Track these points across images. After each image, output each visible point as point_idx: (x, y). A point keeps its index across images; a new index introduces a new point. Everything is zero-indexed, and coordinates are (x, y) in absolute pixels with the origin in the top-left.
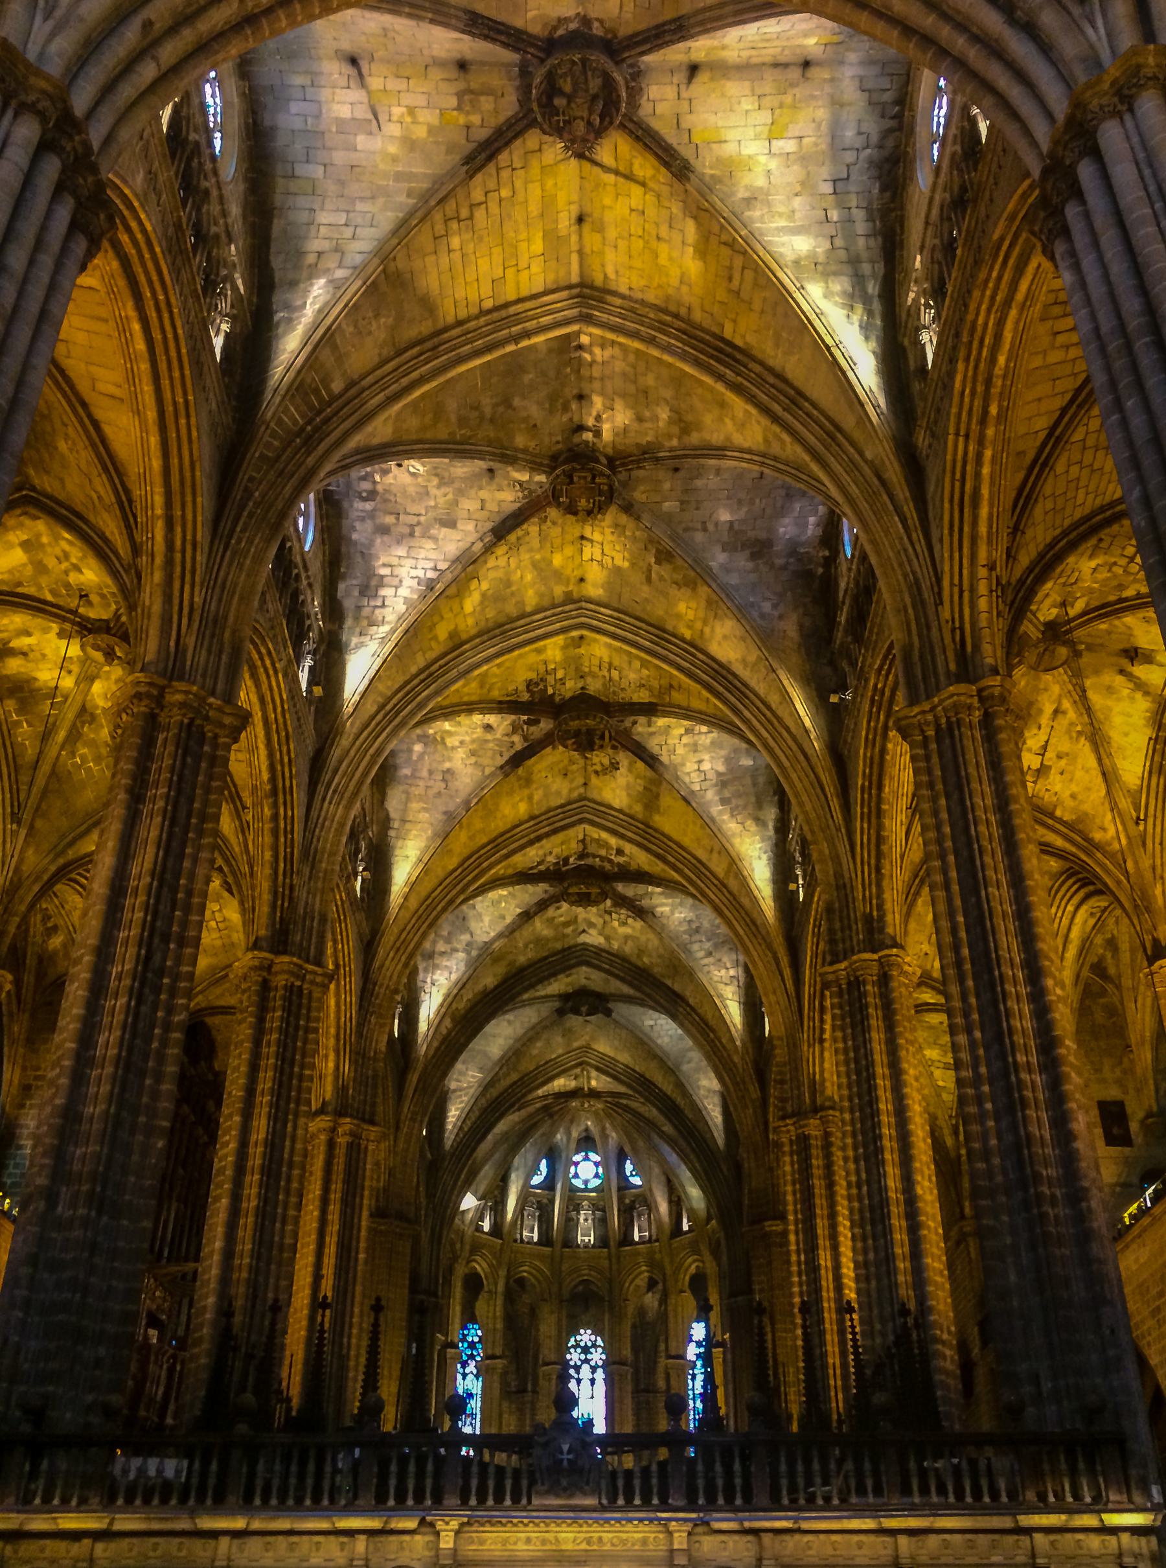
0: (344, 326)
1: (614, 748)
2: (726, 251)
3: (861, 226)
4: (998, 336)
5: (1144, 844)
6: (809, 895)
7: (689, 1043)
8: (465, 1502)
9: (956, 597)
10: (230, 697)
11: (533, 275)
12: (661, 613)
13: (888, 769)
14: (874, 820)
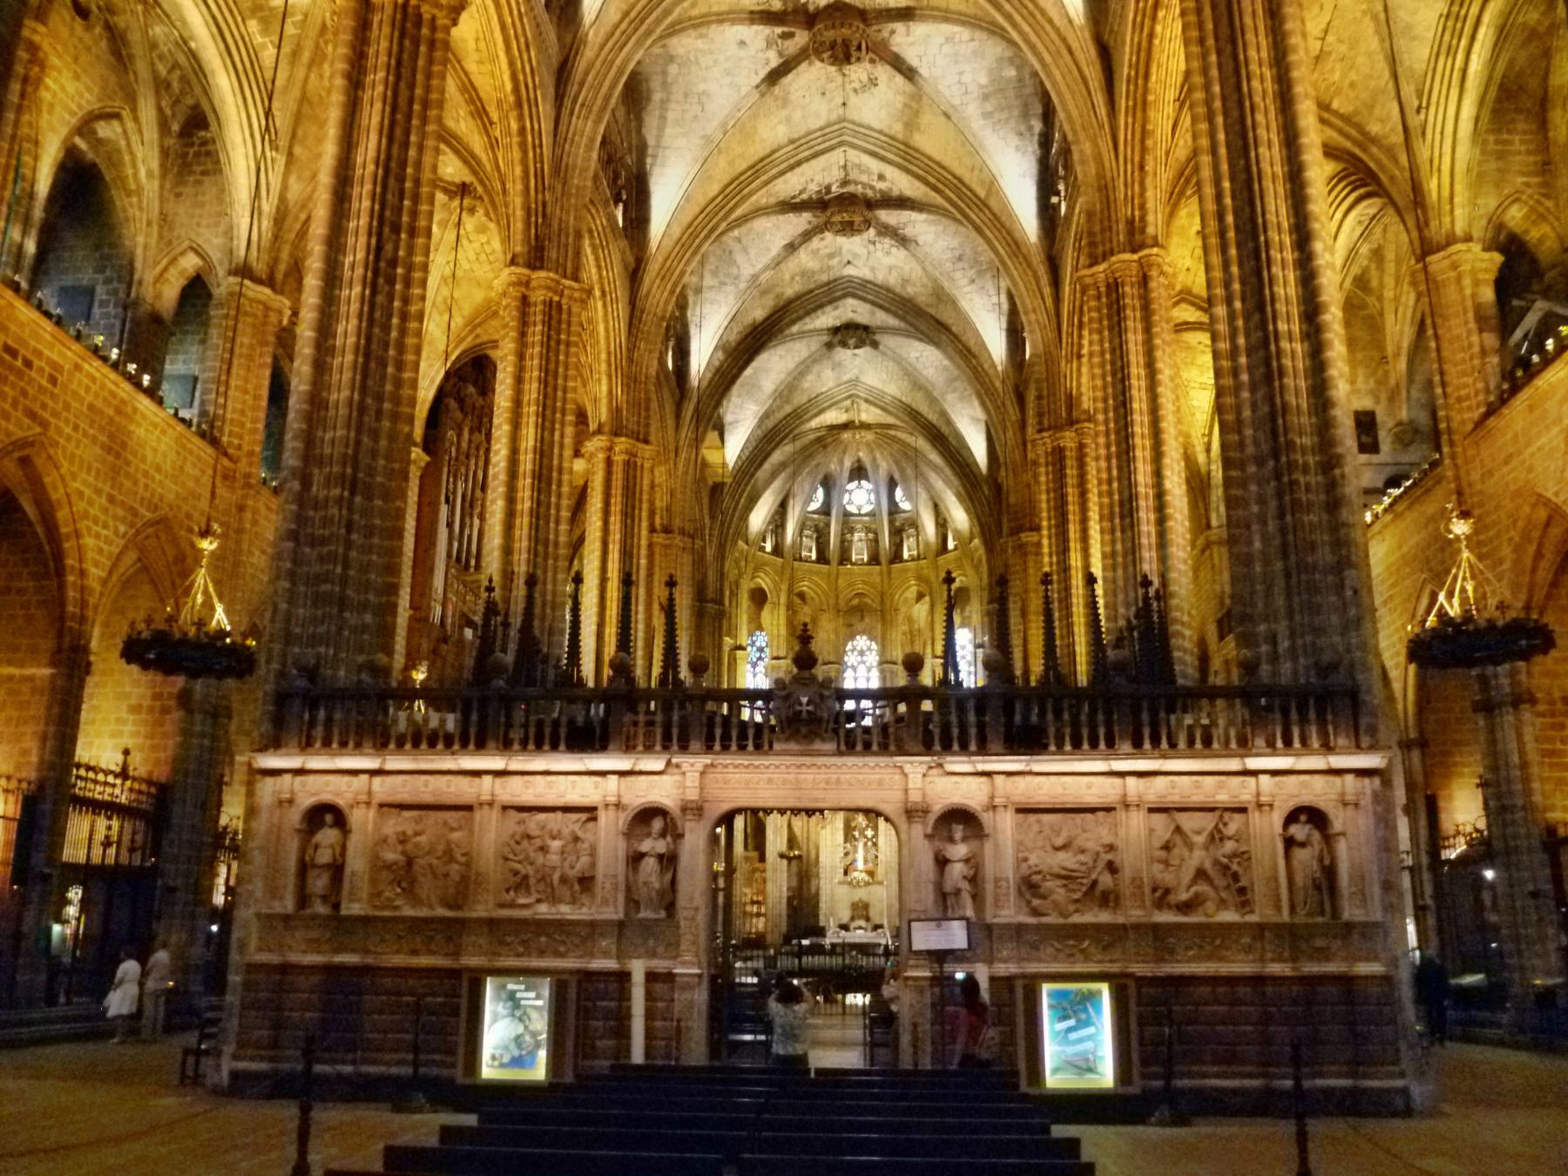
1: (872, 61)
5: (1424, 134)
6: (1071, 208)
8: (709, 749)
13: (1155, 55)
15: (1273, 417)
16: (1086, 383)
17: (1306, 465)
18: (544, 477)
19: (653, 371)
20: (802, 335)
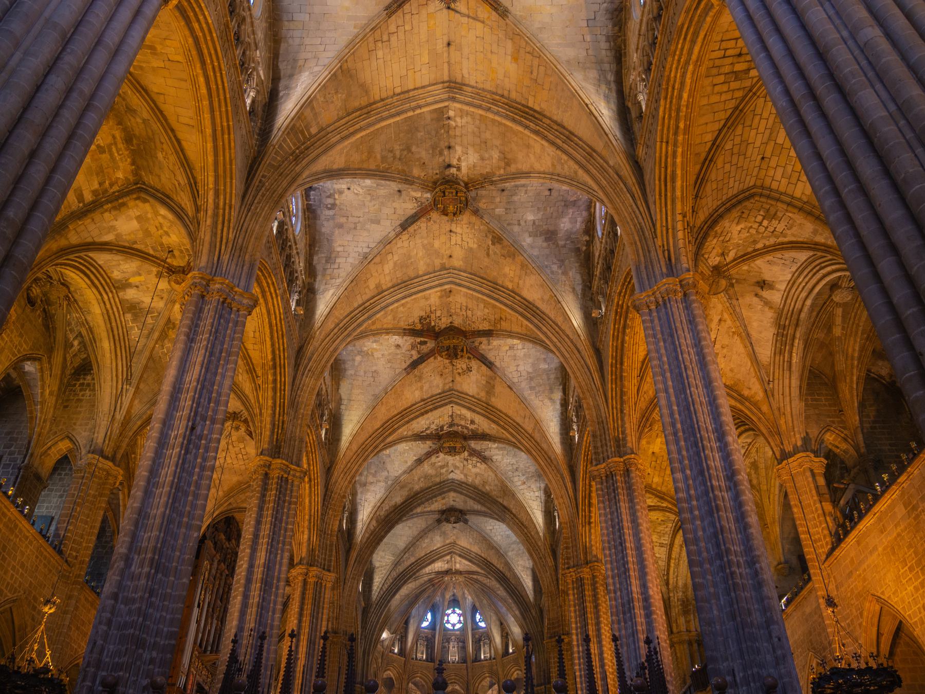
0: (318, 97)
1: (469, 358)
2: (529, 57)
3: (604, 45)
4: (682, 84)
7: (514, 538)
9: (665, 232)
10: (247, 288)
11: (423, 76)
12: (495, 274)
14: (619, 383)
15: (715, 535)
16: (595, 537)
17: (738, 561)
18: (267, 584)
19: (336, 528)
20: (422, 514)
